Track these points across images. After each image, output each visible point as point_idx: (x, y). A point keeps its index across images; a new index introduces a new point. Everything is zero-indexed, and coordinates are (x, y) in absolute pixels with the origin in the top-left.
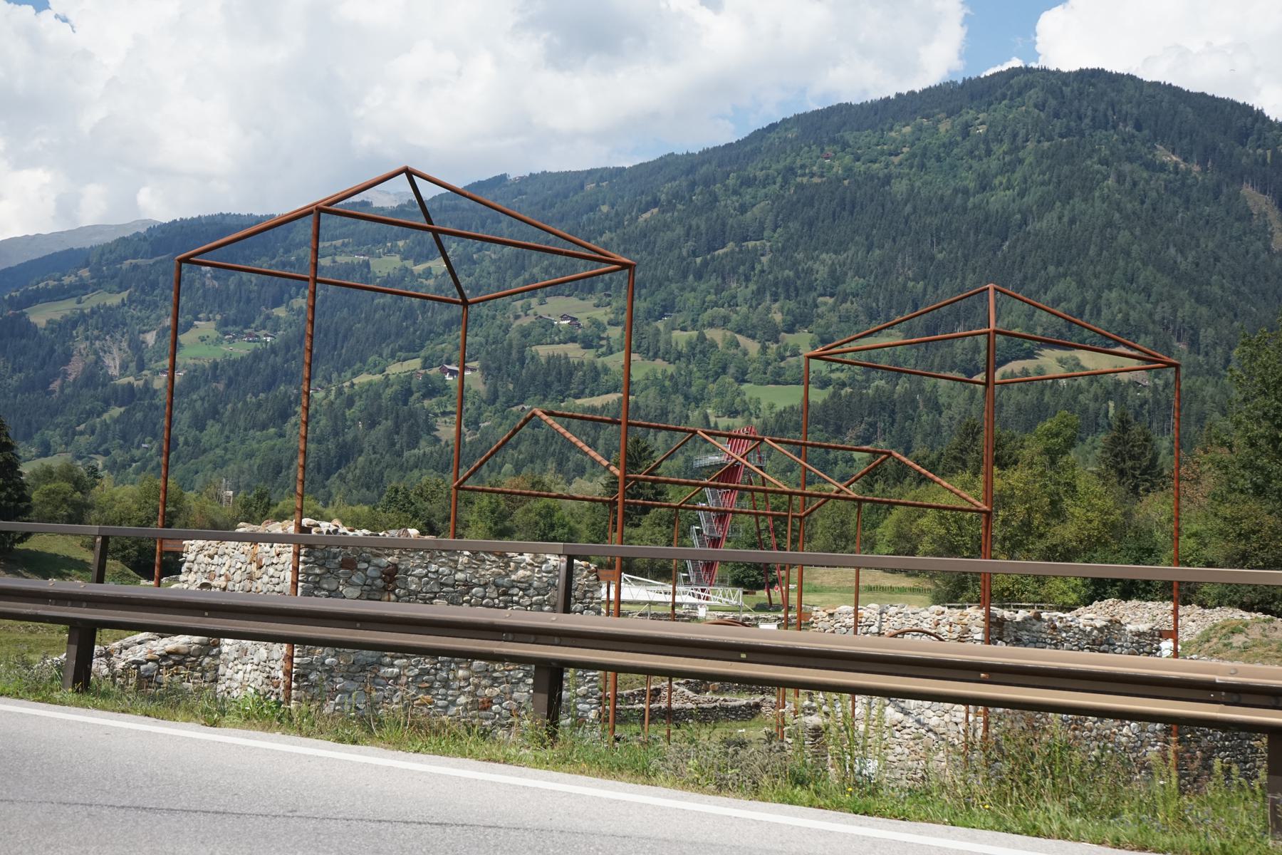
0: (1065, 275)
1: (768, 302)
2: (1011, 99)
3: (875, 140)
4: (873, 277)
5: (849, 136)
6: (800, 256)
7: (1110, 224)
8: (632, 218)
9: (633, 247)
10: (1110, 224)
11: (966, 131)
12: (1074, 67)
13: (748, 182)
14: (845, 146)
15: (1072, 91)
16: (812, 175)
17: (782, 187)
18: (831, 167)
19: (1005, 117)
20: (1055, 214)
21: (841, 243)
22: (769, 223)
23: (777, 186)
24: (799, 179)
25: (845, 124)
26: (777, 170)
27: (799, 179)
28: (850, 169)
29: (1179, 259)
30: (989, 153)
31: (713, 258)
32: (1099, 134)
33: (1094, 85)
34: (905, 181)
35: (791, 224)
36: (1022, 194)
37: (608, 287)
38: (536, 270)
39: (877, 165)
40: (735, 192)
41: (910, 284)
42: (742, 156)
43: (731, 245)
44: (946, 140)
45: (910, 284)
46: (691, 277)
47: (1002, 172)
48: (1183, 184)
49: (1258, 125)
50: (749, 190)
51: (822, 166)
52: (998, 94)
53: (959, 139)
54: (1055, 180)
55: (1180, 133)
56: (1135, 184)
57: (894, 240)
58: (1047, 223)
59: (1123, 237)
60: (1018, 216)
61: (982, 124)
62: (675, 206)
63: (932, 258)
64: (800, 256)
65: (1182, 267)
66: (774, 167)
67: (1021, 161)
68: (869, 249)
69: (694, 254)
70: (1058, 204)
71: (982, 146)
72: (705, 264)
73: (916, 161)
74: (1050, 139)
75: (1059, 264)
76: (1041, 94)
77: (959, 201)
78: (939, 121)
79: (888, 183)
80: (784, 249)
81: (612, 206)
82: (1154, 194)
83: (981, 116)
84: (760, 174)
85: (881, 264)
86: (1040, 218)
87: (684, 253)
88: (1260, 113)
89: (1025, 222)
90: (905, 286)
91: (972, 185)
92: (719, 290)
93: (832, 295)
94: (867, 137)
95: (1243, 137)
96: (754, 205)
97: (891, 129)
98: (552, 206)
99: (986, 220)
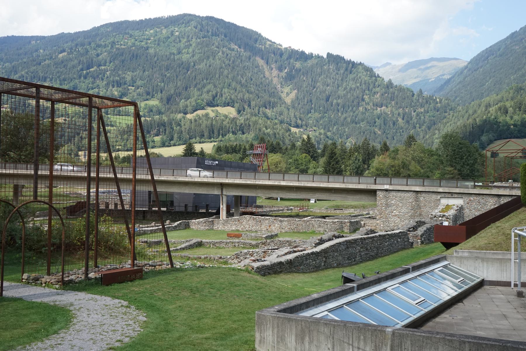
1: (111, 88)
2: (186, 24)
3: (141, 34)
4: (146, 81)
5: (131, 32)
7: (221, 68)
8: (56, 56)
9: (59, 66)
10: (221, 68)
11: (172, 33)
12: (205, 16)
13: (99, 46)
14: (131, 36)
15: (205, 23)
16: (121, 45)
17: (111, 48)
18: (127, 43)
19: (185, 30)
20: (204, 64)
21: (134, 69)
22: (108, 61)
23: (109, 48)
24: (117, 46)
25: (128, 27)
26: (109, 42)
27: (117, 46)
28: (134, 44)
30: (180, 41)
31: (90, 71)
32: (214, 38)
33: (211, 22)
34: (153, 49)
35: (116, 62)
36: (193, 56)
38: (23, 73)
39: (143, 43)
40: (94, 49)
41: (159, 84)
42: (92, 36)
43: (95, 67)
44: (166, 36)
45: (159, 84)
46: (82, 78)
47: (185, 48)
48: (240, 55)
49: (260, 38)
50: (100, 49)
51: (124, 42)
52: (181, 21)
53: (170, 36)
54: (203, 52)
55: (237, 39)
56: (227, 55)
57: (152, 69)
58: (202, 66)
59: (226, 72)
60: (193, 63)
61: (176, 31)
62: (73, 52)
63: (166, 76)
64: (120, 72)
65: (243, 82)
66: (107, 41)
67: (191, 45)
68: (144, 71)
69: (82, 70)
70: (205, 60)
71: (177, 39)
72: (87, 74)
73: (156, 43)
74: (200, 39)
75: (207, 80)
76: (195, 23)
77: (172, 57)
78: (162, 30)
79: (148, 49)
80: (114, 70)
81: (44, 50)
82: (233, 58)
83: (176, 29)
84: (103, 44)
85: (149, 76)
86: (200, 64)
87: (79, 69)
88: (260, 34)
89: (194, 65)
90: (158, 84)
91: (175, 52)
92: (93, 83)
93: (133, 86)
94: (137, 33)
95: (256, 41)
96: (101, 54)
97: (146, 31)
98: (21, 49)
99: (182, 64)
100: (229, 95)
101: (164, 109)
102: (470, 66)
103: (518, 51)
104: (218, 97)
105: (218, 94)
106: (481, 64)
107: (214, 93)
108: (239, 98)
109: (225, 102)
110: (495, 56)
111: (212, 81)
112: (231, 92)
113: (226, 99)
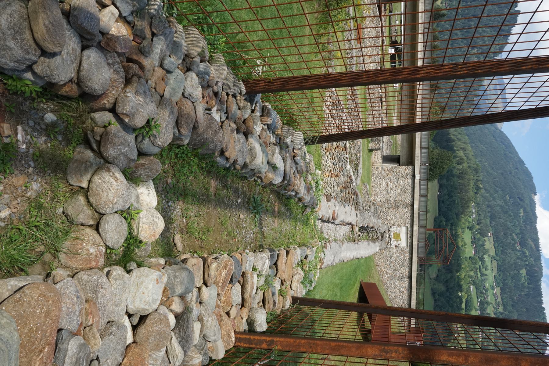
102: (498, 131)
103: (508, 167)
106: (498, 139)
110: (505, 150)
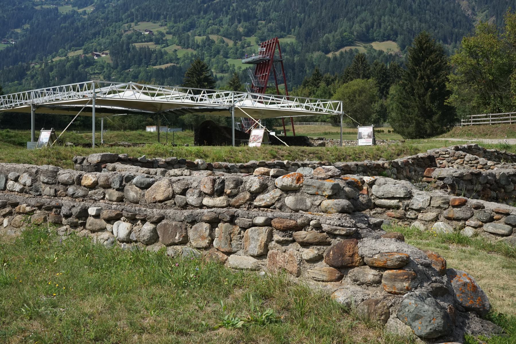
0: (365, 10)
6: (250, 3)
29: (413, 3)
31: (212, 4)
37: (165, 18)
38: (133, 10)
41: (298, 15)
46: (202, 13)
64: (250, 3)
65: (414, 7)
72: (208, 7)
75: (362, 5)
85: (286, 5)
92: (215, 18)
93: (264, 20)
100: (389, 25)
101: (300, 48)
104: (375, 28)
105: (375, 24)
107: (369, 23)
108: (405, 28)
109: (384, 34)
111: (369, 7)
112: (395, 20)
113: (385, 29)
